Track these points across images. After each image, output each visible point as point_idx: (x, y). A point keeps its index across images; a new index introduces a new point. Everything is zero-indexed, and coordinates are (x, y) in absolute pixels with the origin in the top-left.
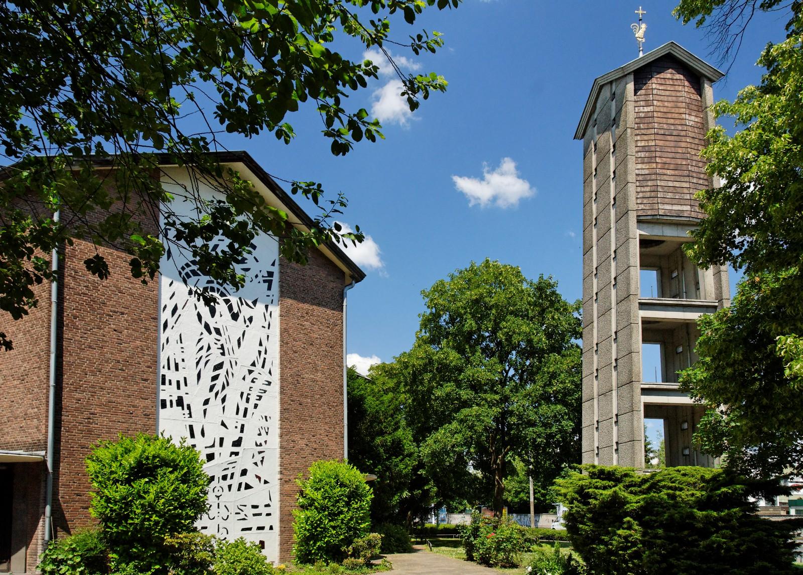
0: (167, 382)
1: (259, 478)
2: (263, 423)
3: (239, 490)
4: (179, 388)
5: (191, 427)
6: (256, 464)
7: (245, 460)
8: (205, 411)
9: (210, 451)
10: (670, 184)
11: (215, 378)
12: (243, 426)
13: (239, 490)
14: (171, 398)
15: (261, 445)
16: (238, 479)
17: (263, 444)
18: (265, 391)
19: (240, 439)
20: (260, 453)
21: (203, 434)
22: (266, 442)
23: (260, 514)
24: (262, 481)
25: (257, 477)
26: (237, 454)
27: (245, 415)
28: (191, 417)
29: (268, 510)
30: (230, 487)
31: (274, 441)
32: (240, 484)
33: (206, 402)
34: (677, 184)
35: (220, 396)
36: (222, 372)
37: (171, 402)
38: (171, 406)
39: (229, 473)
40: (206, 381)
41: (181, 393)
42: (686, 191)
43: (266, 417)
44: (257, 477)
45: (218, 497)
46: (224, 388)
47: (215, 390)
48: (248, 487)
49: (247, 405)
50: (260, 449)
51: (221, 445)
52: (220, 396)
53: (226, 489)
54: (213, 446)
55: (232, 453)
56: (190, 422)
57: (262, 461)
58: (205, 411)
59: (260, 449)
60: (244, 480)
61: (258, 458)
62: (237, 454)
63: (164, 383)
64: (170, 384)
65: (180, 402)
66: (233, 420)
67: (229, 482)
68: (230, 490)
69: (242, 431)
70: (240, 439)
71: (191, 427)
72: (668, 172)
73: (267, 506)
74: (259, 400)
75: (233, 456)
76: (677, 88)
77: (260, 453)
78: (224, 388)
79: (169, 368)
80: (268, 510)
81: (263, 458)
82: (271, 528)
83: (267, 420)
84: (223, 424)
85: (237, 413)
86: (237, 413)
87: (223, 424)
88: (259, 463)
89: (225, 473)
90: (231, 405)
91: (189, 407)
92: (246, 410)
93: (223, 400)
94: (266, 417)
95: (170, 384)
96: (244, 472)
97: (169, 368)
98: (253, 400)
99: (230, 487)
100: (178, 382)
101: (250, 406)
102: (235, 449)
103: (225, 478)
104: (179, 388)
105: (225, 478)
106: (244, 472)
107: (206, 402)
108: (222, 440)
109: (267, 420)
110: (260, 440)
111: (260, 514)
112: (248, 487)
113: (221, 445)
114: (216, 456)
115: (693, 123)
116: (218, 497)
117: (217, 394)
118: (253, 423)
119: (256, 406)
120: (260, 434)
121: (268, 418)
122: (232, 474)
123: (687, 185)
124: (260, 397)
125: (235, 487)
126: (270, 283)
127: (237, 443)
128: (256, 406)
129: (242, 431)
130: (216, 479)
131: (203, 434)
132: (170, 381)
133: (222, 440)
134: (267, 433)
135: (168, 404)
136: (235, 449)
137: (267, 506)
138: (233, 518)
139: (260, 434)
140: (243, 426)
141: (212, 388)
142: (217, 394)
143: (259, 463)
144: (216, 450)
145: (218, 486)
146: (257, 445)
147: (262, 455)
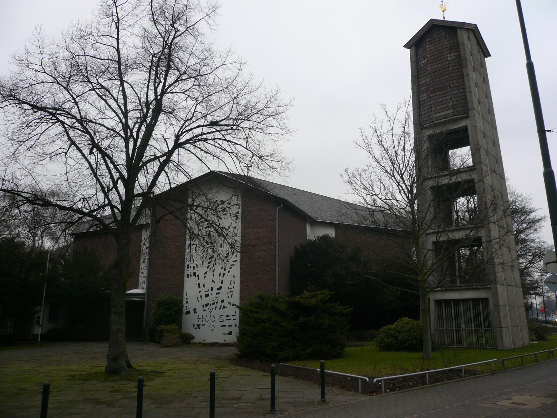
0: (189, 267)
1: (230, 303)
2: (233, 279)
3: (220, 309)
4: (194, 269)
5: (199, 284)
6: (228, 297)
7: (223, 296)
8: (205, 277)
9: (207, 293)
10: (440, 100)
11: (209, 263)
12: (222, 281)
13: (220, 309)
14: (191, 273)
15: (231, 289)
16: (220, 304)
17: (232, 288)
18: (234, 265)
19: (221, 287)
20: (230, 292)
21: (204, 286)
22: (233, 287)
23: (230, 319)
24: (232, 304)
25: (229, 303)
26: (219, 293)
27: (223, 276)
28: (199, 280)
29: (234, 318)
30: (216, 308)
31: (237, 286)
32: (221, 307)
33: (206, 273)
34: (444, 99)
35: (212, 270)
36: (213, 259)
37: (191, 275)
38: (191, 276)
39: (215, 302)
40: (206, 264)
41: (195, 271)
42: (450, 101)
43: (234, 276)
44: (229, 303)
45: (210, 312)
46: (214, 266)
47: (210, 268)
48: (224, 307)
49: (224, 272)
50: (231, 290)
51: (212, 290)
52: (212, 270)
53: (214, 308)
54: (208, 291)
55: (217, 293)
56: (198, 282)
57: (231, 296)
58: (205, 277)
59: (231, 290)
60: (223, 304)
61: (230, 295)
62: (219, 293)
63: (188, 268)
64: (191, 268)
65: (194, 274)
66: (217, 279)
67: (215, 305)
68: (216, 309)
69: (222, 283)
70: (221, 287)
71: (199, 284)
72: (438, 93)
73: (234, 315)
74: (231, 269)
75: (218, 294)
76: (441, 41)
77: (230, 292)
78: (214, 266)
79: (190, 262)
80: (234, 318)
81: (232, 294)
82: (236, 326)
83: (234, 277)
84: (213, 281)
85: (220, 276)
86: (220, 276)
87: (213, 281)
88: (230, 297)
89: (213, 302)
90: (217, 273)
91: (198, 276)
92: (224, 274)
93: (213, 271)
94: (234, 276)
95: (191, 268)
96: (223, 301)
97: (190, 262)
98: (227, 270)
99: (216, 308)
100: (194, 267)
101: (226, 272)
102: (219, 291)
103: (213, 304)
104: (194, 269)
105: (213, 304)
106: (223, 301)
107: (206, 273)
108: (212, 288)
109: (234, 277)
110: (231, 286)
111: (230, 319)
112: (224, 307)
113: (212, 290)
114: (210, 295)
115: (453, 57)
116: (210, 312)
117: (210, 269)
118: (228, 279)
119: (229, 272)
120: (231, 284)
121: (235, 276)
122: (217, 302)
123: (450, 97)
124: (231, 268)
125: (218, 308)
126: (237, 217)
127: (220, 289)
128: (229, 272)
129: (222, 283)
130: (209, 304)
131: (204, 286)
132: (191, 267)
133: (212, 288)
134: (234, 283)
135: (190, 275)
136: (219, 291)
137: (234, 315)
138: (218, 321)
139: (231, 284)
140: (222, 281)
141: (208, 267)
142: (210, 269)
143: (230, 297)
144: (210, 292)
145: (210, 307)
146: (229, 289)
147: (232, 293)
